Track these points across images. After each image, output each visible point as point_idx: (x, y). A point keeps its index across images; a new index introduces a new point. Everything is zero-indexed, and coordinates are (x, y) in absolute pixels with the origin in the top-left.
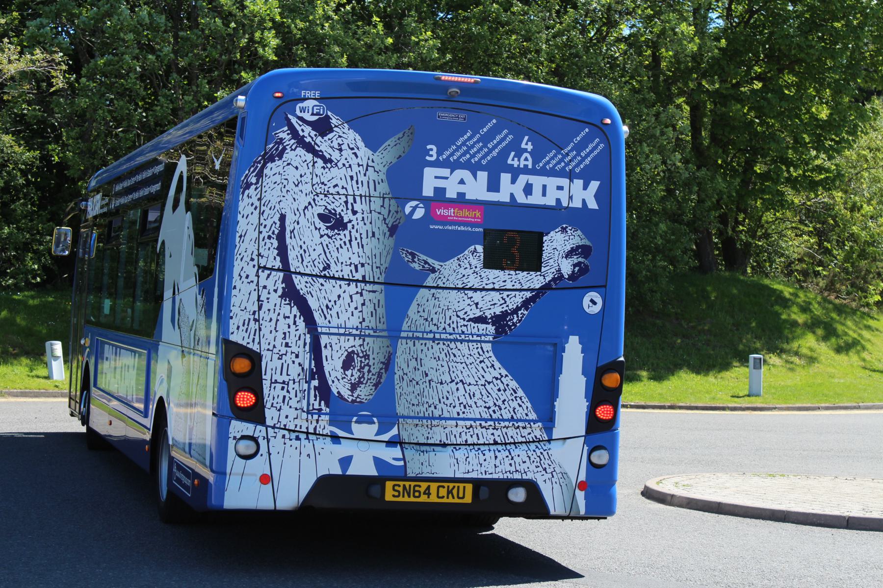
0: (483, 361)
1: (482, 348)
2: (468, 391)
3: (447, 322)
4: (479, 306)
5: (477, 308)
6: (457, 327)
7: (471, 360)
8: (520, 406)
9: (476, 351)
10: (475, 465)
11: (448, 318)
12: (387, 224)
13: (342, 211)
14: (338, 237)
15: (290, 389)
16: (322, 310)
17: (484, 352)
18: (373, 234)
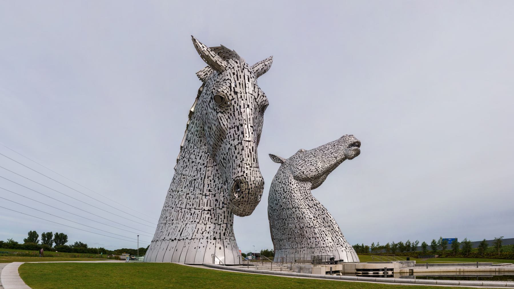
0: (307, 198)
1: (306, 192)
2: (301, 211)
4: (304, 173)
5: (303, 174)
6: (294, 184)
7: (302, 198)
9: (304, 194)
10: (306, 244)
11: (290, 180)
12: (257, 102)
13: (228, 92)
14: (227, 112)
15: (212, 213)
16: (221, 162)
17: (308, 194)
18: (248, 106)
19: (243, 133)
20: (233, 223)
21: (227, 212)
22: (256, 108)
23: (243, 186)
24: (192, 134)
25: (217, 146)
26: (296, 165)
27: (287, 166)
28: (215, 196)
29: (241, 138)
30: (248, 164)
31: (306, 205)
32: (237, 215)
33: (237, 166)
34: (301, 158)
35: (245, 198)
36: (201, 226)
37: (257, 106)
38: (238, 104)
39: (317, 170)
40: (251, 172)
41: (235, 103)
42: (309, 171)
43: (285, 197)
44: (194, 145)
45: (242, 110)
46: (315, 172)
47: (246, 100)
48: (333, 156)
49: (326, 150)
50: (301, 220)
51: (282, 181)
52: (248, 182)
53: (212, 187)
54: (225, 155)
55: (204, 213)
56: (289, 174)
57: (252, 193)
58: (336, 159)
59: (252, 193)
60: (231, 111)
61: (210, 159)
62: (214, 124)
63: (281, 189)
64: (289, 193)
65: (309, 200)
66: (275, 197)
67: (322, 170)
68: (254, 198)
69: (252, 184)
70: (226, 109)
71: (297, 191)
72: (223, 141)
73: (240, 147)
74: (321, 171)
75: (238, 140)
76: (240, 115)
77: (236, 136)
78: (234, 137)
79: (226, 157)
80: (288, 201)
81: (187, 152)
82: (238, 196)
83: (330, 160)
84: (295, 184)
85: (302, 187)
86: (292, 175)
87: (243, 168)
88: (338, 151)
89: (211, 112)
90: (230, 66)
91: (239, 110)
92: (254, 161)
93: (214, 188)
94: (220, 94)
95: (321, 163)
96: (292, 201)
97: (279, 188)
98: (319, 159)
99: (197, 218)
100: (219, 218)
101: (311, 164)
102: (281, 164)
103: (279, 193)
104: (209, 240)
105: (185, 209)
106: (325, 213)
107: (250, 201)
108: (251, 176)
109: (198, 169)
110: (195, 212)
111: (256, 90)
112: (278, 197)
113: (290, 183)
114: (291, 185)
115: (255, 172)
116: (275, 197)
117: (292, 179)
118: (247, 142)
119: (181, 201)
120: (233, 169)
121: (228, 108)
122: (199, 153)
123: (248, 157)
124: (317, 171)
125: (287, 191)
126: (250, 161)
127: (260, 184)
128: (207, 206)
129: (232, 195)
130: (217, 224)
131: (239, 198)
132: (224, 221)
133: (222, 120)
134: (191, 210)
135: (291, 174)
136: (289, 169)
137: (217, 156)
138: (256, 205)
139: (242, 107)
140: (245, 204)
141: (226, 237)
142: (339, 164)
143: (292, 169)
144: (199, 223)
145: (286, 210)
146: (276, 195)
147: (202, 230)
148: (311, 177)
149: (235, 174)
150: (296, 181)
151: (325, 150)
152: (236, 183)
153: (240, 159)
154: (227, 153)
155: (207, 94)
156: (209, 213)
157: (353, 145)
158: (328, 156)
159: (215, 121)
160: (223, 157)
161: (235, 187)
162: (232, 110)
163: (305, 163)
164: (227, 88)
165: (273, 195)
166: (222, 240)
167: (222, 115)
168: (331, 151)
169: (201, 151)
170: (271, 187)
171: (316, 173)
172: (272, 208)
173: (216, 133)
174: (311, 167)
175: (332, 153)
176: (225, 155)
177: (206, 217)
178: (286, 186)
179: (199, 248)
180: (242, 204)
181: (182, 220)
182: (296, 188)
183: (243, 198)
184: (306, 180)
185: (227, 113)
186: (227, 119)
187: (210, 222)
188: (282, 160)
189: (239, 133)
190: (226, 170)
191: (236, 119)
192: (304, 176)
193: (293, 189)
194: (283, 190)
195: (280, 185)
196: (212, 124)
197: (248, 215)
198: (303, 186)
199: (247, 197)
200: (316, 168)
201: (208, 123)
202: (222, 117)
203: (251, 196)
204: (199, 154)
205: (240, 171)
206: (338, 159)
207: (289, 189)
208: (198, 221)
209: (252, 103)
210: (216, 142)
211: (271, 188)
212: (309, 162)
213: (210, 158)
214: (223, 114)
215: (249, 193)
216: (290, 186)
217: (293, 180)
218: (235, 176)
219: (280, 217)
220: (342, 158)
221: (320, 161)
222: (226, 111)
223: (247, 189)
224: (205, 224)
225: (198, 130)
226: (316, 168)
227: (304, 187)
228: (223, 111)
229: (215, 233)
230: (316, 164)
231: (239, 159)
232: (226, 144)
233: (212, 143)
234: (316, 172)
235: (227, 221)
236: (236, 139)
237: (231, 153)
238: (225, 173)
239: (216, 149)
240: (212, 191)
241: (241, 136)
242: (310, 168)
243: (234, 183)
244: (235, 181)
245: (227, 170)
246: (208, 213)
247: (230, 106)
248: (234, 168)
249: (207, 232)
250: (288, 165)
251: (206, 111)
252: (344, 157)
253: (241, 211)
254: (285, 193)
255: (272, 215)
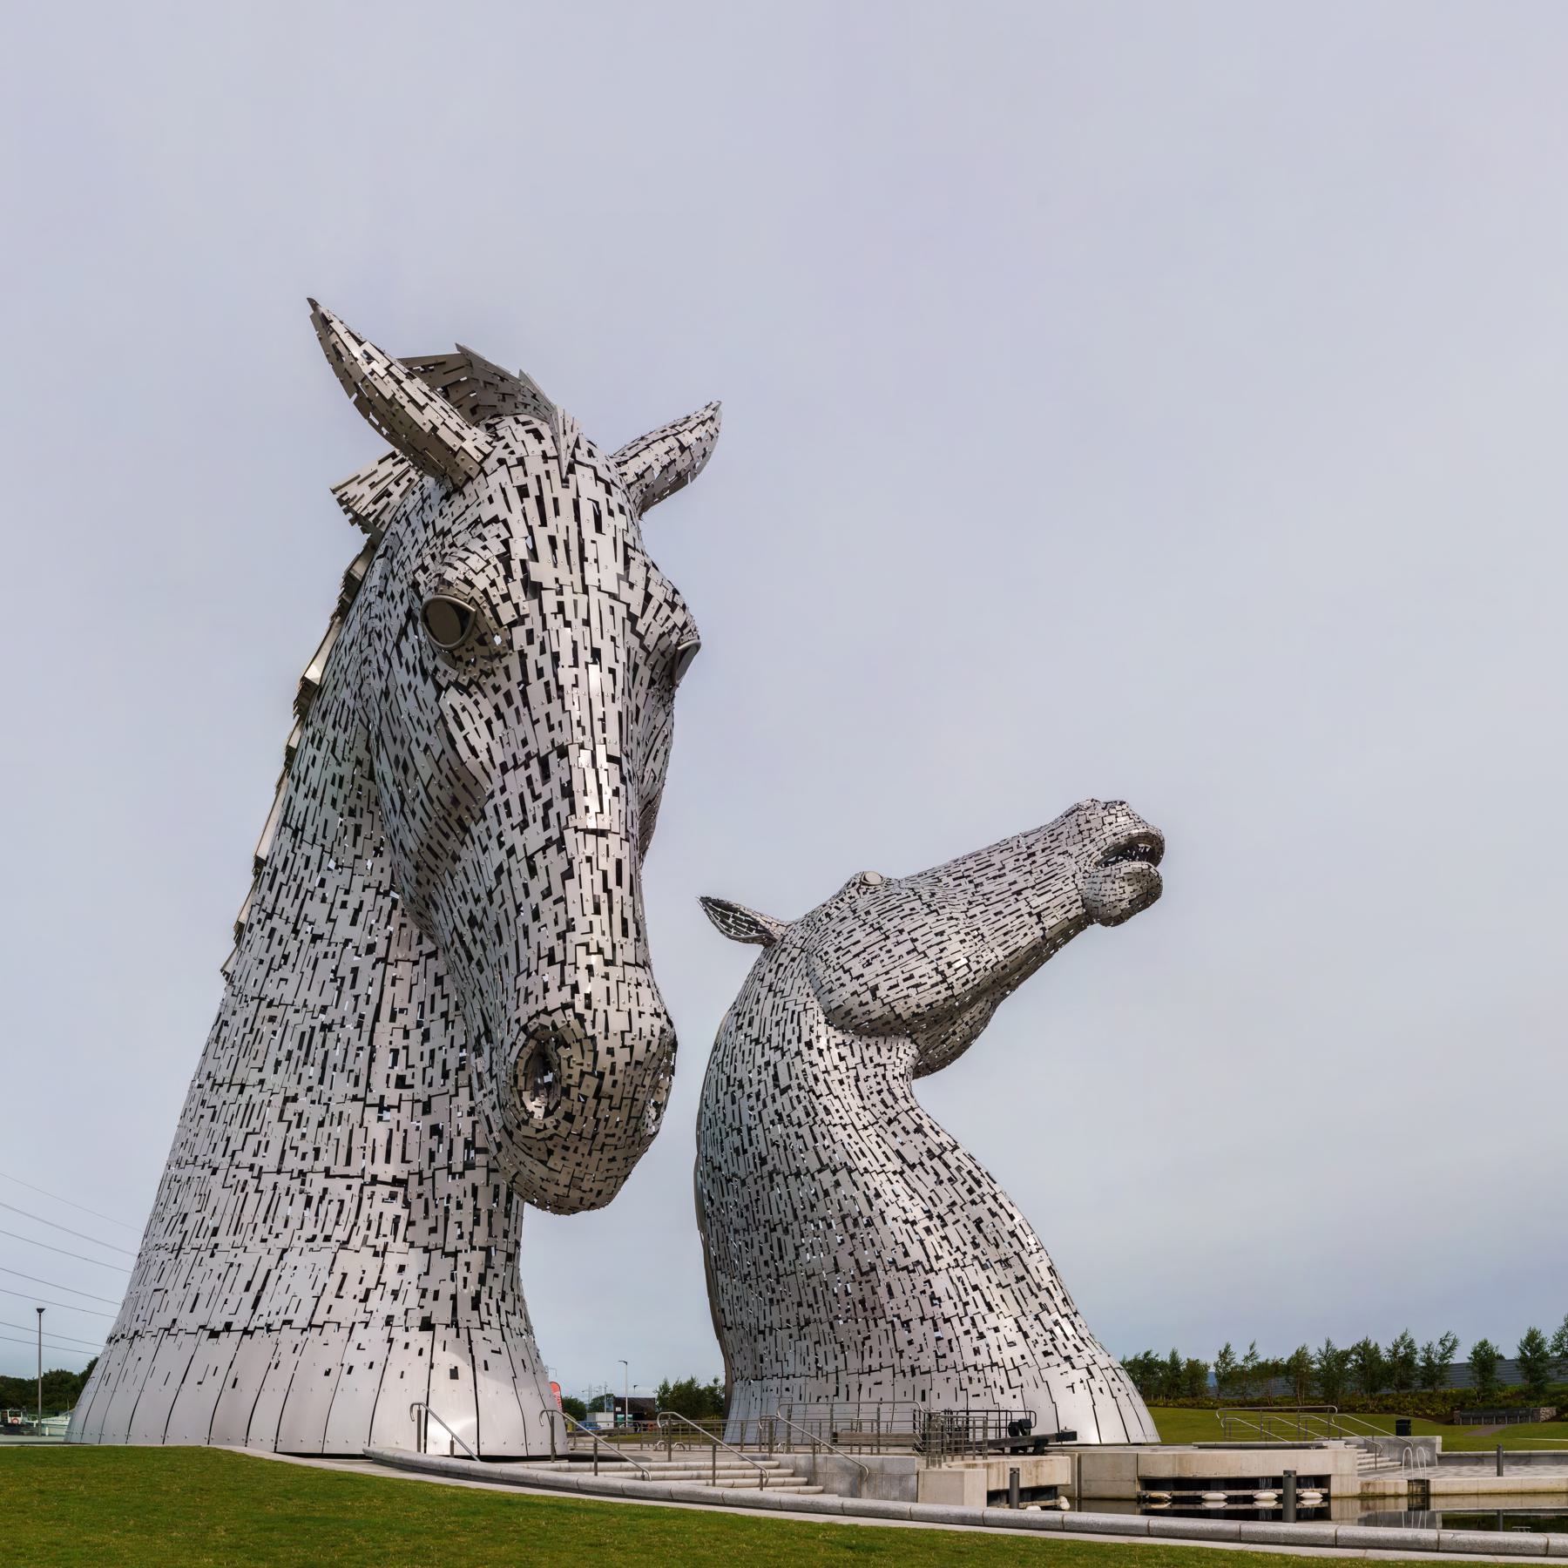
3: (805, 1038)
4: (879, 994)
6: (829, 1048)
8: (994, 1215)
12: (641, 637)
13: (493, 584)
15: (412, 1196)
16: (461, 936)
18: (596, 654)
19: (567, 791)
20: (517, 1244)
21: (491, 1188)
22: (636, 667)
23: (569, 1059)
24: (314, 796)
25: (436, 856)
26: (836, 951)
27: (793, 960)
28: (427, 1109)
29: (558, 814)
30: (593, 949)
31: (887, 1157)
32: (538, 1206)
33: (539, 958)
34: (863, 917)
35: (579, 1120)
36: (357, 1262)
37: (642, 654)
38: (542, 644)
39: (944, 981)
40: (608, 989)
41: (530, 641)
42: (903, 985)
43: (784, 1115)
44: (323, 851)
45: (566, 676)
46: (933, 986)
47: (587, 623)
48: (1025, 910)
49: (990, 875)
50: (861, 1232)
51: (768, 1032)
52: (593, 1038)
53: (413, 1066)
54: (477, 900)
55: (371, 1198)
56: (805, 999)
57: (617, 1092)
58: (1040, 921)
59: (617, 1092)
60: (509, 679)
61: (404, 920)
62: (422, 748)
63: (760, 1073)
64: (802, 1094)
65: (904, 1128)
66: (729, 1116)
67: (971, 976)
68: (625, 1119)
69: (617, 1051)
70: (485, 669)
71: (841, 1082)
72: (466, 830)
73: (554, 862)
74: (964, 985)
75: (546, 826)
76: (556, 702)
77: (534, 808)
78: (524, 811)
79: (485, 911)
80: (798, 1137)
81: (285, 889)
82: (547, 1108)
83: (1009, 928)
84: (835, 1051)
85: (870, 1065)
86: (816, 1005)
87: (569, 969)
88: (1052, 881)
89: (410, 686)
90: (504, 454)
91: (548, 675)
92: (625, 933)
93: (424, 1069)
94: (455, 596)
95: (963, 941)
96: (819, 1137)
97: (750, 1067)
98: (953, 922)
99: (337, 1223)
100: (450, 1223)
101: (915, 949)
102: (756, 950)
103: (749, 1096)
104: (398, 1333)
105: (275, 1178)
106: (982, 1197)
107: (607, 1136)
108: (612, 1009)
109: (345, 971)
110: (325, 1190)
111: (637, 573)
112: (746, 1112)
113: (809, 1045)
114: (815, 1052)
115: (633, 989)
116: (729, 1116)
117: (818, 1023)
118: (591, 838)
119: (258, 1138)
120: (519, 973)
121: (496, 663)
122: (347, 892)
123: (597, 911)
124: (945, 985)
125: (794, 1083)
126: (603, 933)
127: (653, 1048)
128: (388, 1160)
129: (515, 1105)
130: (436, 1249)
131: (550, 1122)
132: (471, 1234)
133: (461, 728)
134: (308, 1183)
135: (812, 998)
136: (804, 972)
137: (437, 909)
138: (637, 1157)
139: (566, 658)
140: (580, 1151)
141: (485, 1318)
142: (1056, 947)
143: (819, 972)
144: (350, 1246)
145: (786, 1178)
146: (736, 1106)
147: (360, 1283)
148: (915, 1015)
149: (532, 999)
150: (838, 1033)
151: (983, 879)
152: (532, 1043)
153: (556, 923)
154: (490, 893)
155: (389, 593)
156: (400, 1198)
157: (1126, 850)
158: (1000, 907)
159: (429, 729)
160: (471, 912)
161: (527, 1062)
162: (517, 675)
163: (883, 943)
164: (488, 562)
165: (721, 1105)
166: (463, 1333)
167: (465, 699)
168: (1015, 882)
169: (358, 882)
170: (713, 1066)
171: (939, 993)
172: (714, 1168)
173: (434, 791)
174: (913, 964)
175: (1019, 893)
176: (481, 905)
177: (381, 1214)
178: (787, 1058)
179: (349, 1372)
180: (567, 1148)
181: (262, 1231)
182: (836, 1068)
183: (569, 1117)
184: (886, 1028)
185: (489, 691)
186: (489, 723)
187: (405, 1240)
188: (767, 926)
189: (550, 790)
190: (482, 978)
191: (535, 722)
192: (877, 1010)
193: (821, 1077)
194: (770, 1082)
195: (758, 1054)
196: (414, 744)
197: (592, 1206)
198: (872, 1061)
199: (589, 1113)
200: (936, 969)
201: (395, 740)
202: (464, 709)
203: (611, 1108)
204: (346, 898)
205: (553, 986)
206: (1049, 922)
207: (801, 1076)
208: (340, 1234)
209: (613, 639)
210: (431, 837)
211: (709, 1068)
212: (901, 938)
213: (404, 915)
214: (470, 696)
215: (598, 1095)
216: (806, 1059)
217: (821, 1029)
218: (532, 1008)
219: (757, 1216)
220: (1071, 915)
221: (958, 932)
222: (483, 680)
223: (591, 1074)
224: (380, 1249)
225: (342, 778)
226: (940, 969)
227: (879, 1065)
228: (471, 682)
229: (430, 1295)
230: (936, 949)
231: (551, 923)
232: (485, 849)
233: (411, 843)
234: (936, 989)
235: (490, 1235)
236: (535, 821)
237: (508, 894)
238: (477, 992)
239: (433, 872)
240: (411, 1086)
241: (561, 806)
242: (908, 968)
243: (524, 1046)
244: (530, 1036)
245: (491, 980)
246: (393, 1196)
247: (505, 655)
248: (523, 966)
249: (389, 1289)
250: (795, 953)
251: (384, 678)
252: (1080, 911)
253: (558, 1184)
254: (781, 1095)
255: (717, 1204)
